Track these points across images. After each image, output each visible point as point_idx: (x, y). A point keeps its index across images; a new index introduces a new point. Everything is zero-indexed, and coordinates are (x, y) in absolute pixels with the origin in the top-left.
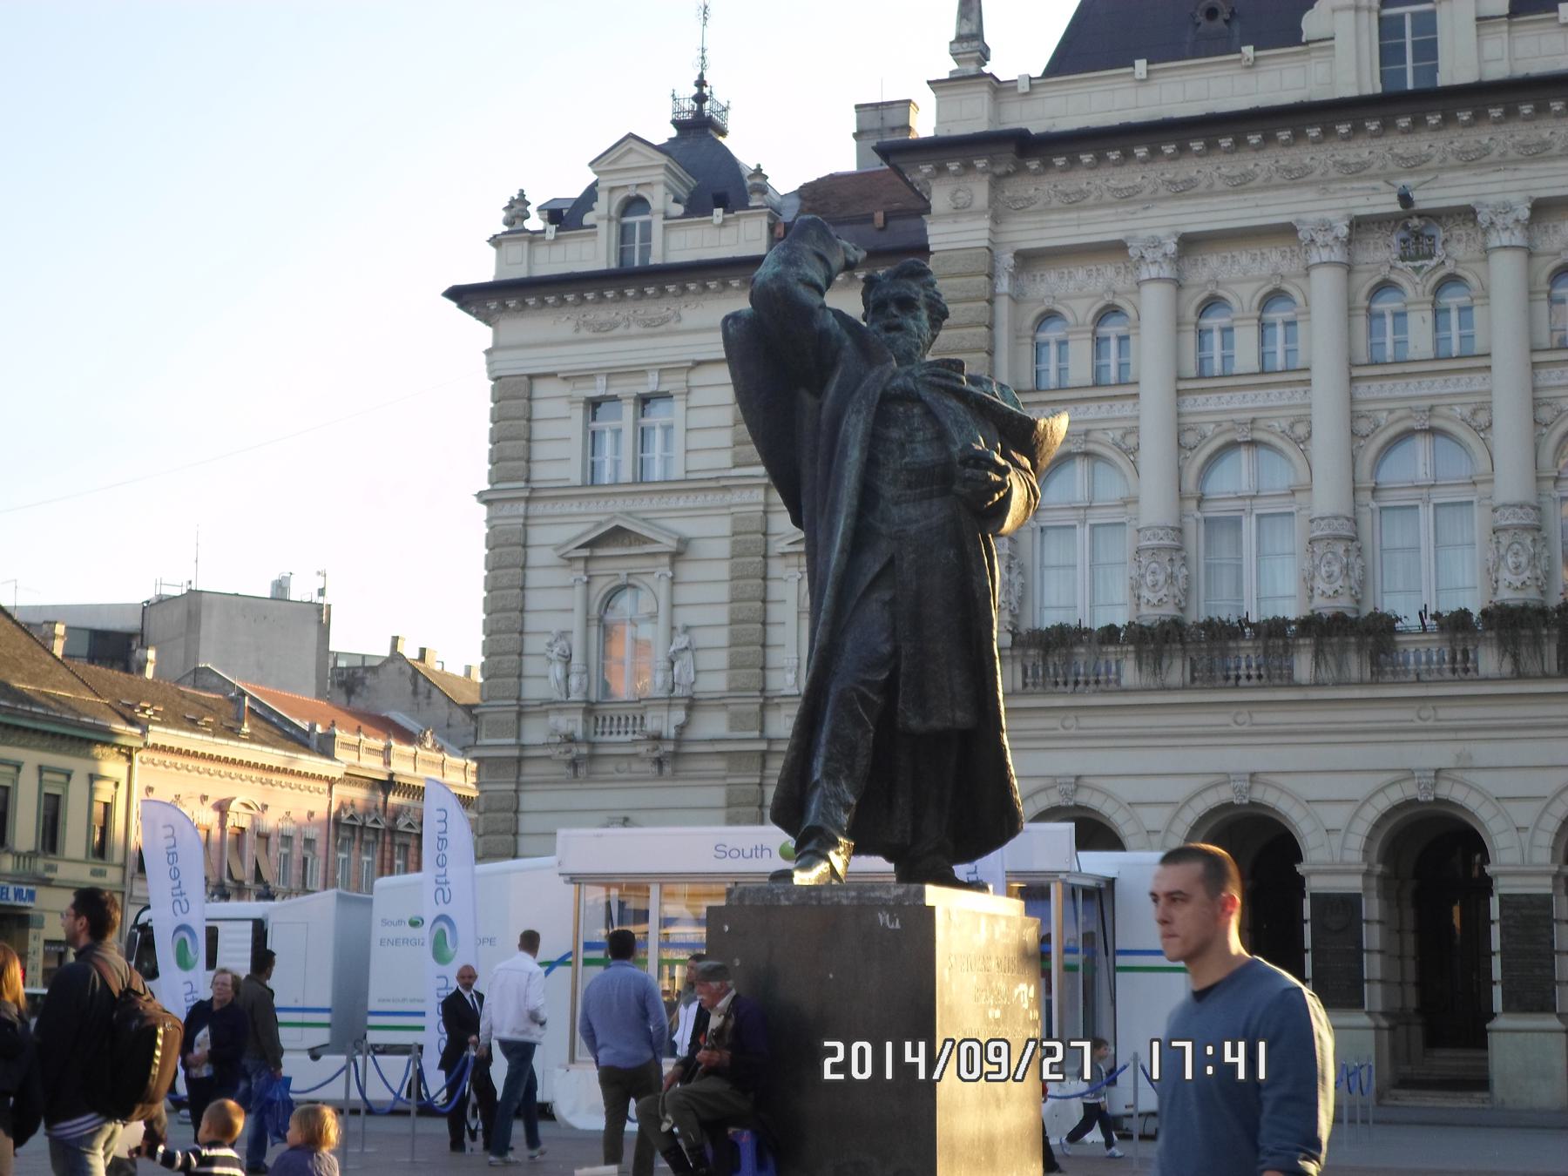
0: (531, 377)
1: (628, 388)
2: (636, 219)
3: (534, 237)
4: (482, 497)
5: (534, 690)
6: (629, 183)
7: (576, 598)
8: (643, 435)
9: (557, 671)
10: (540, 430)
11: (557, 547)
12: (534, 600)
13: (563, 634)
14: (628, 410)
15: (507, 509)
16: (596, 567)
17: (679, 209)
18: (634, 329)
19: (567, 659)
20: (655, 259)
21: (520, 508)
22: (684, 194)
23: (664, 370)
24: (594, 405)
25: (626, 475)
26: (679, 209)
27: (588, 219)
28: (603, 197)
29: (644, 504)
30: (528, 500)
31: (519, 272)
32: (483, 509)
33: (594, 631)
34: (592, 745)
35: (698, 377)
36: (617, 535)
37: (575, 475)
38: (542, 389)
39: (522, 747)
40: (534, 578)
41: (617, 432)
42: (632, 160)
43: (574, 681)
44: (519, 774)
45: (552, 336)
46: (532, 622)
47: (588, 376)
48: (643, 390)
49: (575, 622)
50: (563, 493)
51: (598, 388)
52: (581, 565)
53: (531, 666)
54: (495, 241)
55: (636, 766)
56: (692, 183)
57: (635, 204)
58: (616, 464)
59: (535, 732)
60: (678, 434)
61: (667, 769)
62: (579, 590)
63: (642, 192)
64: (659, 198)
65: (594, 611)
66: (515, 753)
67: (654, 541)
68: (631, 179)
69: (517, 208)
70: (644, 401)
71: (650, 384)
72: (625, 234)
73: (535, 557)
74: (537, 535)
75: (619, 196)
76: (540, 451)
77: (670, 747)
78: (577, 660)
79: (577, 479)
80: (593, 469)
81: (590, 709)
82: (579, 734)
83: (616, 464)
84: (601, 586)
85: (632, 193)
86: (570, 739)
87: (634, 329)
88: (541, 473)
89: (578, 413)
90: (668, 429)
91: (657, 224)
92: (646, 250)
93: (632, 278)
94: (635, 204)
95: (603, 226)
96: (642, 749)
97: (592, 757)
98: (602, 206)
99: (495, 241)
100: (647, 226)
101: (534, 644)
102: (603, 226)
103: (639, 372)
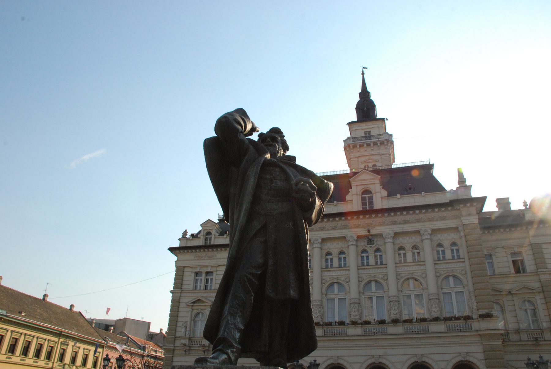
0: (184, 267)
1: (204, 270)
2: (209, 236)
3: (188, 239)
4: (171, 292)
5: (178, 334)
6: (208, 229)
7: (189, 315)
8: (207, 281)
9: (183, 330)
10: (185, 278)
11: (186, 303)
12: (180, 314)
13: (186, 322)
14: (204, 275)
15: (176, 294)
16: (194, 308)
17: (218, 234)
18: (206, 258)
19: (186, 327)
20: (212, 243)
21: (179, 294)
22: (219, 232)
23: (212, 267)
24: (197, 274)
25: (202, 288)
26: (218, 234)
27: (199, 236)
28: (202, 232)
29: (206, 295)
30: (181, 293)
31: (185, 245)
32: (171, 295)
33: (192, 322)
34: (190, 347)
35: (219, 268)
36: (199, 301)
37: (191, 287)
38: (186, 269)
39: (175, 347)
40: (181, 310)
41: (201, 280)
42: (209, 225)
43: (187, 333)
44: (174, 353)
45: (190, 258)
46: (180, 319)
47: (196, 267)
48: (207, 271)
49: (188, 320)
50: (189, 291)
51: (198, 270)
52: (191, 307)
53: (178, 329)
54: (180, 239)
55: (199, 352)
56: (221, 230)
57: (209, 233)
58: (200, 286)
59: (178, 343)
60: (214, 280)
61: (206, 353)
62: (190, 312)
63: (211, 231)
64: (214, 232)
65: (193, 318)
66: (173, 348)
67: (206, 302)
68: (208, 228)
69: (185, 233)
70: (207, 273)
71: (209, 269)
72: (206, 239)
73: (182, 305)
74: (182, 300)
75: (206, 231)
76: (184, 283)
77: (207, 348)
78: (188, 329)
79: (191, 288)
80: (196, 287)
81: (190, 339)
82: (187, 344)
83: (200, 286)
84: (195, 312)
85: (208, 231)
86: (185, 345)
87: (206, 258)
88: (184, 287)
89: (193, 275)
90: (212, 279)
91: (213, 237)
92: (210, 242)
93: (207, 247)
94: (209, 233)
95: (202, 238)
96: (200, 348)
97: (190, 350)
98: (202, 233)
99: (180, 239)
100: (211, 238)
101: (179, 324)
102: (202, 238)
103: (207, 267)
